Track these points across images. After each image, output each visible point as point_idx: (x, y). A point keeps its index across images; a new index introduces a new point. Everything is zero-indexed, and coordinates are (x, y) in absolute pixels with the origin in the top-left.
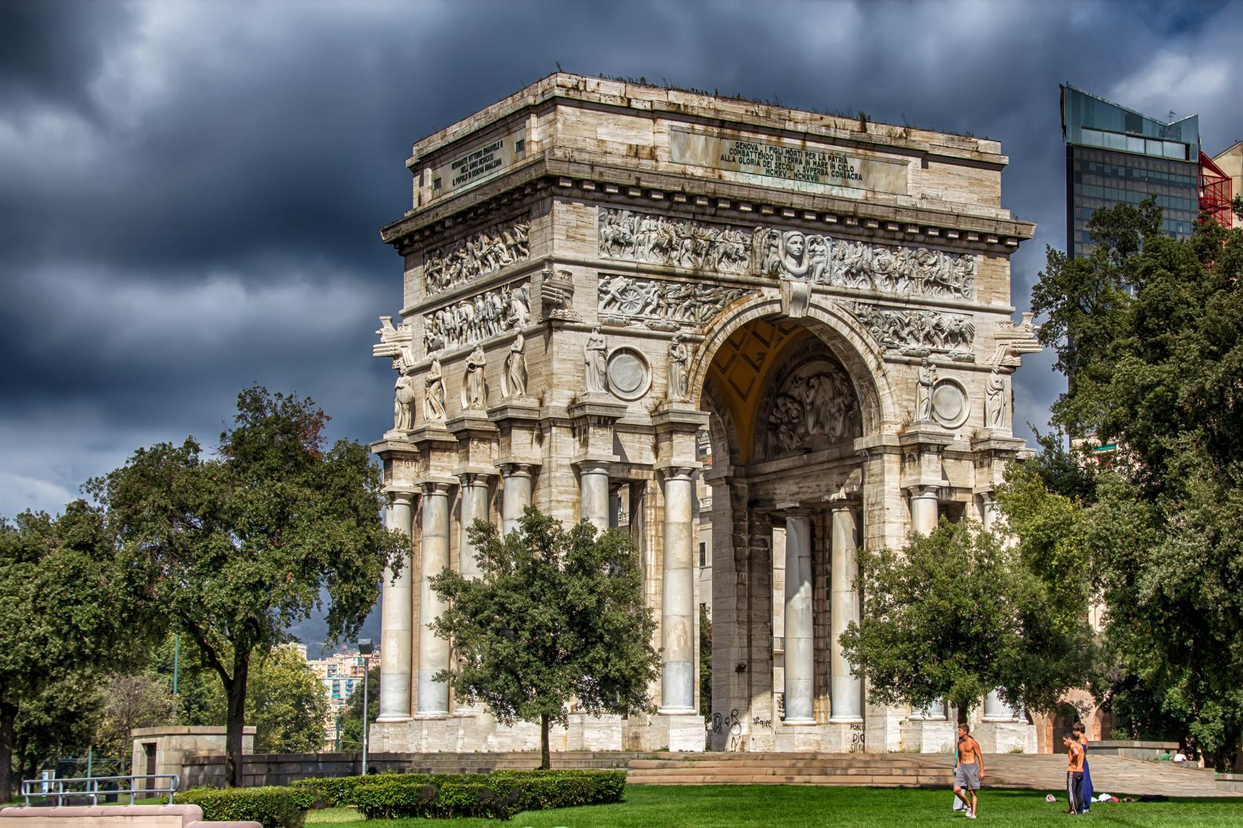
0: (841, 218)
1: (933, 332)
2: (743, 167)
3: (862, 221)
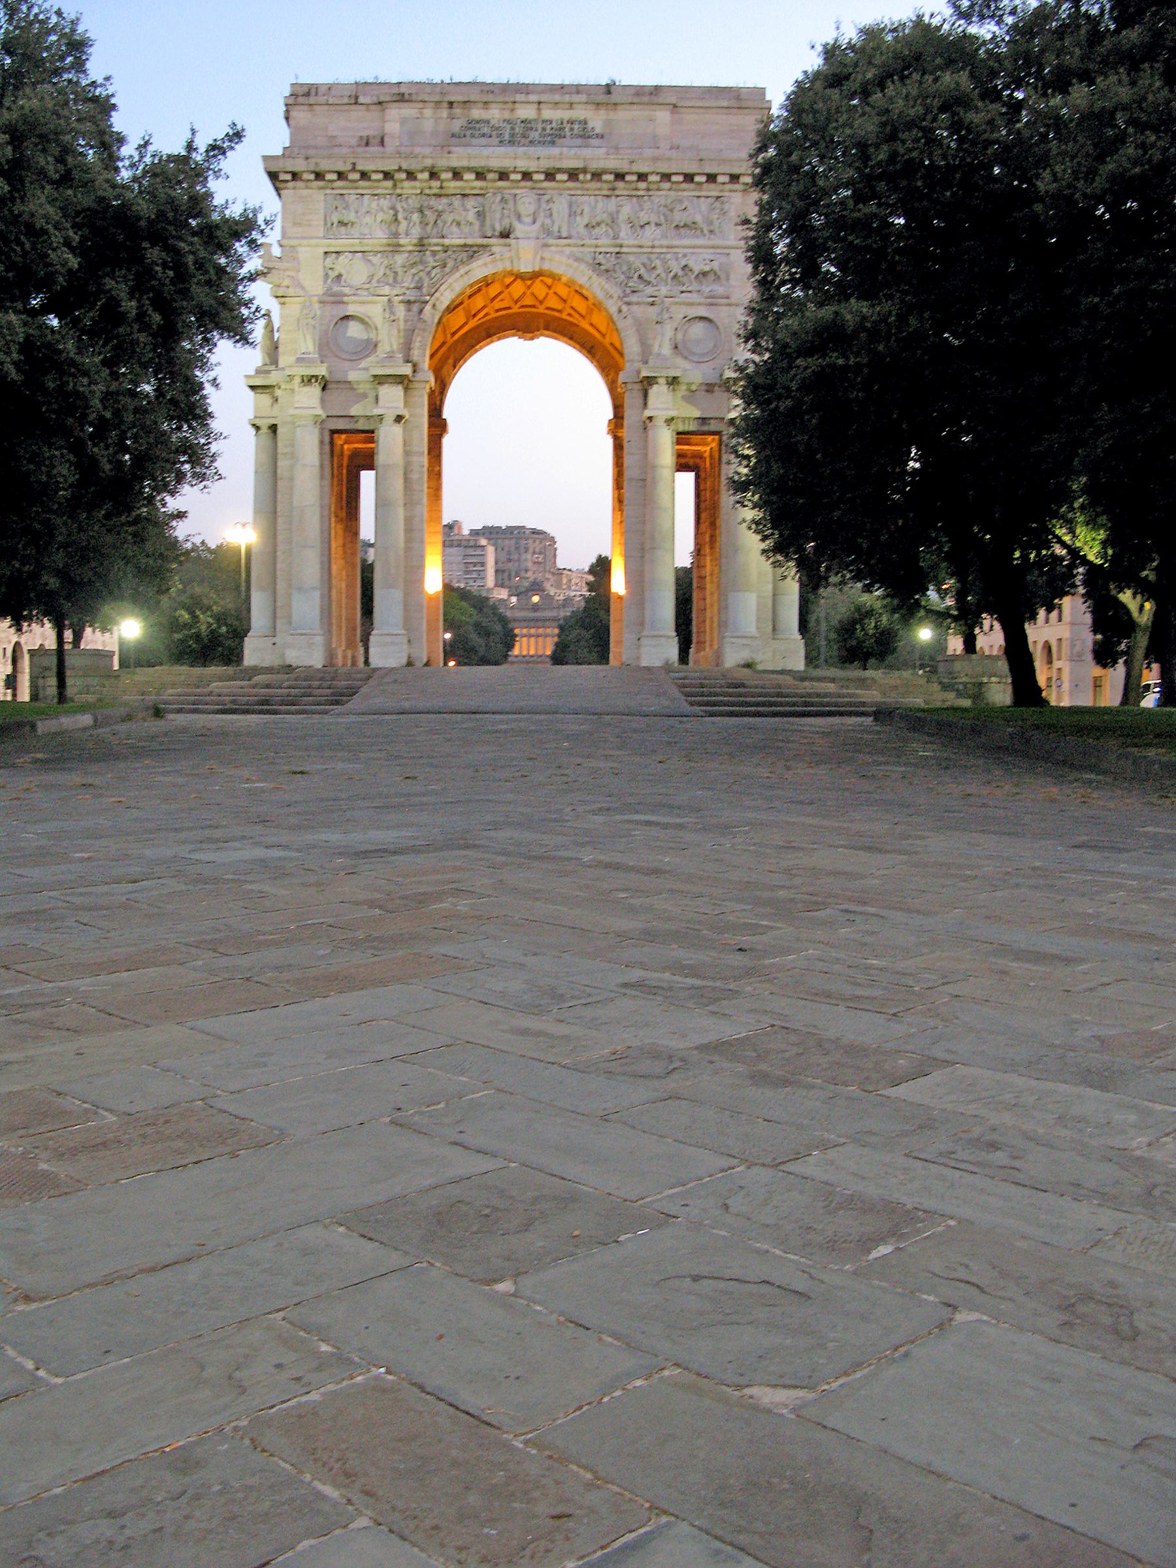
0: (573, 175)
1: (680, 273)
2: (474, 141)
3: (597, 176)
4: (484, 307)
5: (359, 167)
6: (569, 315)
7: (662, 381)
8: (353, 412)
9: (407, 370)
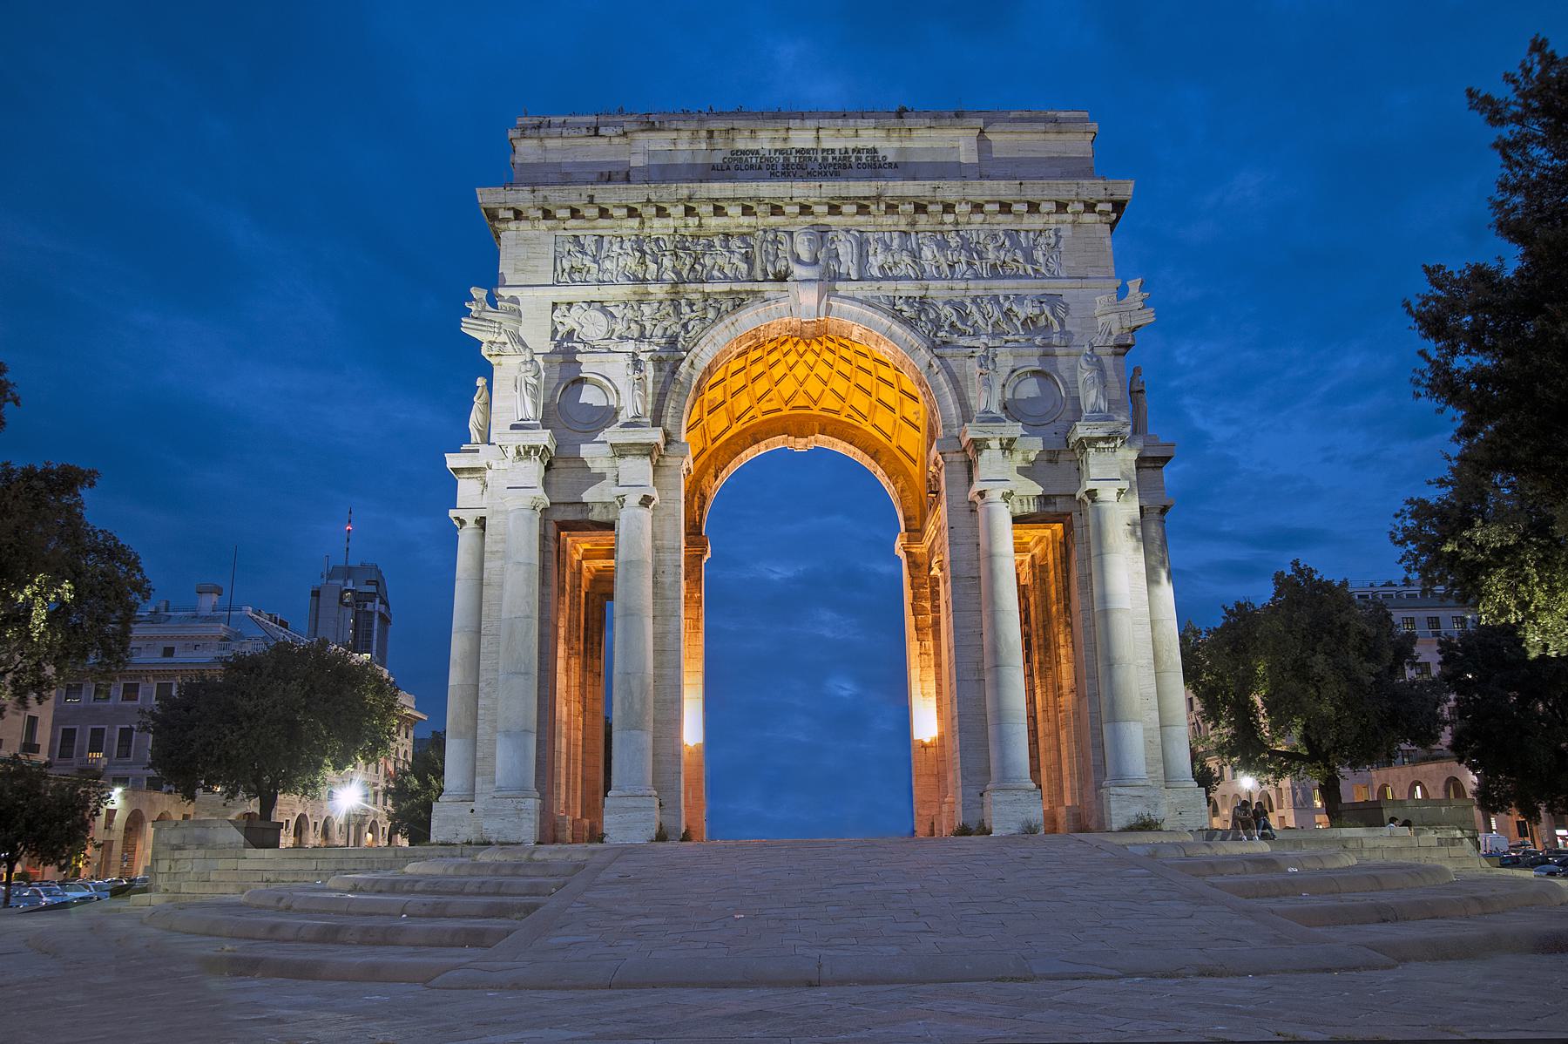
4: (751, 408)
5: (597, 201)
6: (849, 416)
7: (995, 444)
8: (586, 497)
9: (656, 436)
